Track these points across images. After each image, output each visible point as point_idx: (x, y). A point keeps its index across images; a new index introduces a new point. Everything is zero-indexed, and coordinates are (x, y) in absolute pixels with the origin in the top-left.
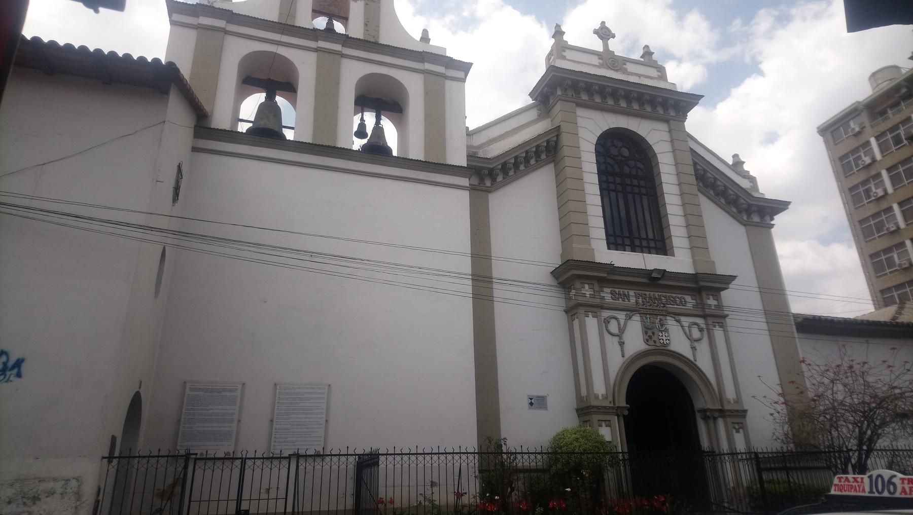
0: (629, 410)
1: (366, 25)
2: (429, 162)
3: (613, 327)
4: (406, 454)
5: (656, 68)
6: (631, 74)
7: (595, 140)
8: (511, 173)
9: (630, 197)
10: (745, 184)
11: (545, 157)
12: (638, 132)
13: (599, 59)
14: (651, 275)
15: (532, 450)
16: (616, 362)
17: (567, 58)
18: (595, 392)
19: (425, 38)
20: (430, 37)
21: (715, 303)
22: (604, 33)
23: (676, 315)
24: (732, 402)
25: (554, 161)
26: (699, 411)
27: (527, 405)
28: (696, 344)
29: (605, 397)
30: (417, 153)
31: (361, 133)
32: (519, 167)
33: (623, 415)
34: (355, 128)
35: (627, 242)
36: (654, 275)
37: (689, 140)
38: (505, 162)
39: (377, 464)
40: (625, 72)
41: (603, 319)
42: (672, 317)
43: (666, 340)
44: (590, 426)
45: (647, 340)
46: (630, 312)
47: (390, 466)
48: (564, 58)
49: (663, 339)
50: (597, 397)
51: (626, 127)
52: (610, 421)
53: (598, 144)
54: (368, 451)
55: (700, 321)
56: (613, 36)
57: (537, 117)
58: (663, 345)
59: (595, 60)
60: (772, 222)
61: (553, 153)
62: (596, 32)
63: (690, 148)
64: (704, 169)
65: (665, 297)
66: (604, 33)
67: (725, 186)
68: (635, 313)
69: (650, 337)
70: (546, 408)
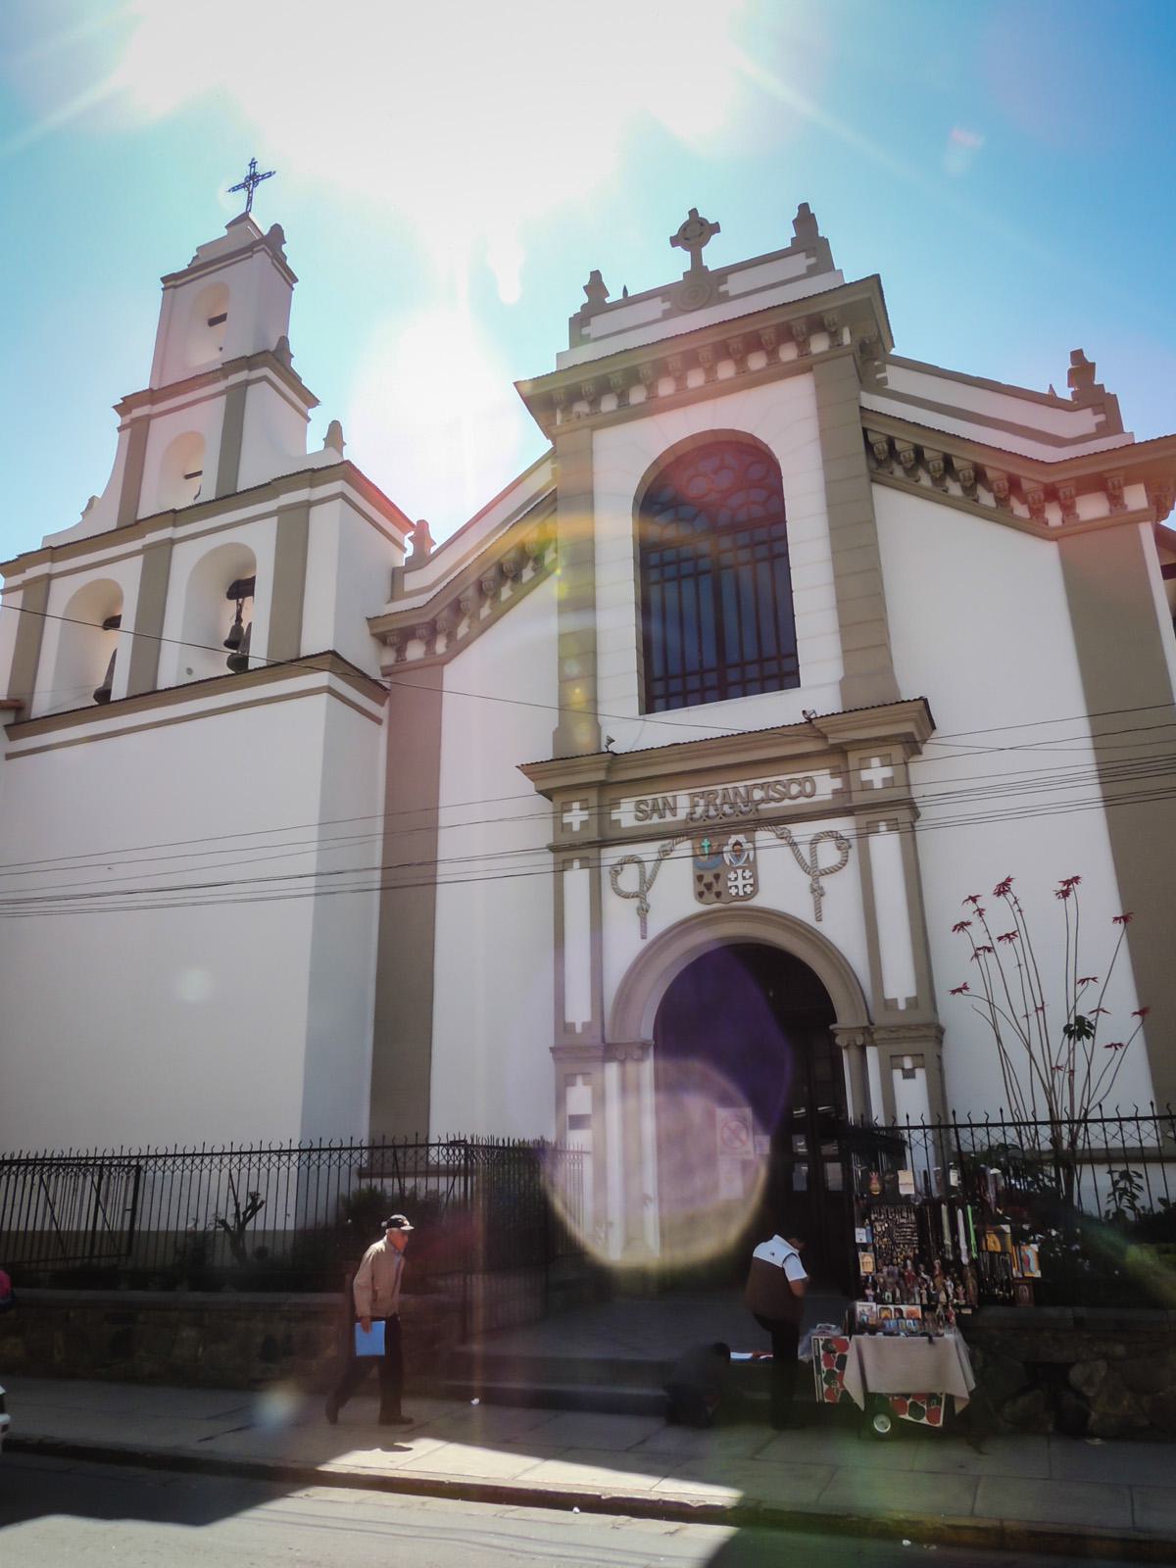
3: (629, 879)
13: (663, 302)
17: (592, 337)
18: (569, 1019)
19: (335, 435)
21: (887, 772)
22: (695, 232)
24: (902, 1006)
28: (825, 881)
29: (586, 1026)
34: (226, 635)
43: (745, 886)
45: (701, 895)
49: (736, 887)
55: (843, 825)
56: (716, 228)
59: (658, 307)
62: (674, 241)
65: (762, 786)
68: (678, 839)
69: (709, 886)
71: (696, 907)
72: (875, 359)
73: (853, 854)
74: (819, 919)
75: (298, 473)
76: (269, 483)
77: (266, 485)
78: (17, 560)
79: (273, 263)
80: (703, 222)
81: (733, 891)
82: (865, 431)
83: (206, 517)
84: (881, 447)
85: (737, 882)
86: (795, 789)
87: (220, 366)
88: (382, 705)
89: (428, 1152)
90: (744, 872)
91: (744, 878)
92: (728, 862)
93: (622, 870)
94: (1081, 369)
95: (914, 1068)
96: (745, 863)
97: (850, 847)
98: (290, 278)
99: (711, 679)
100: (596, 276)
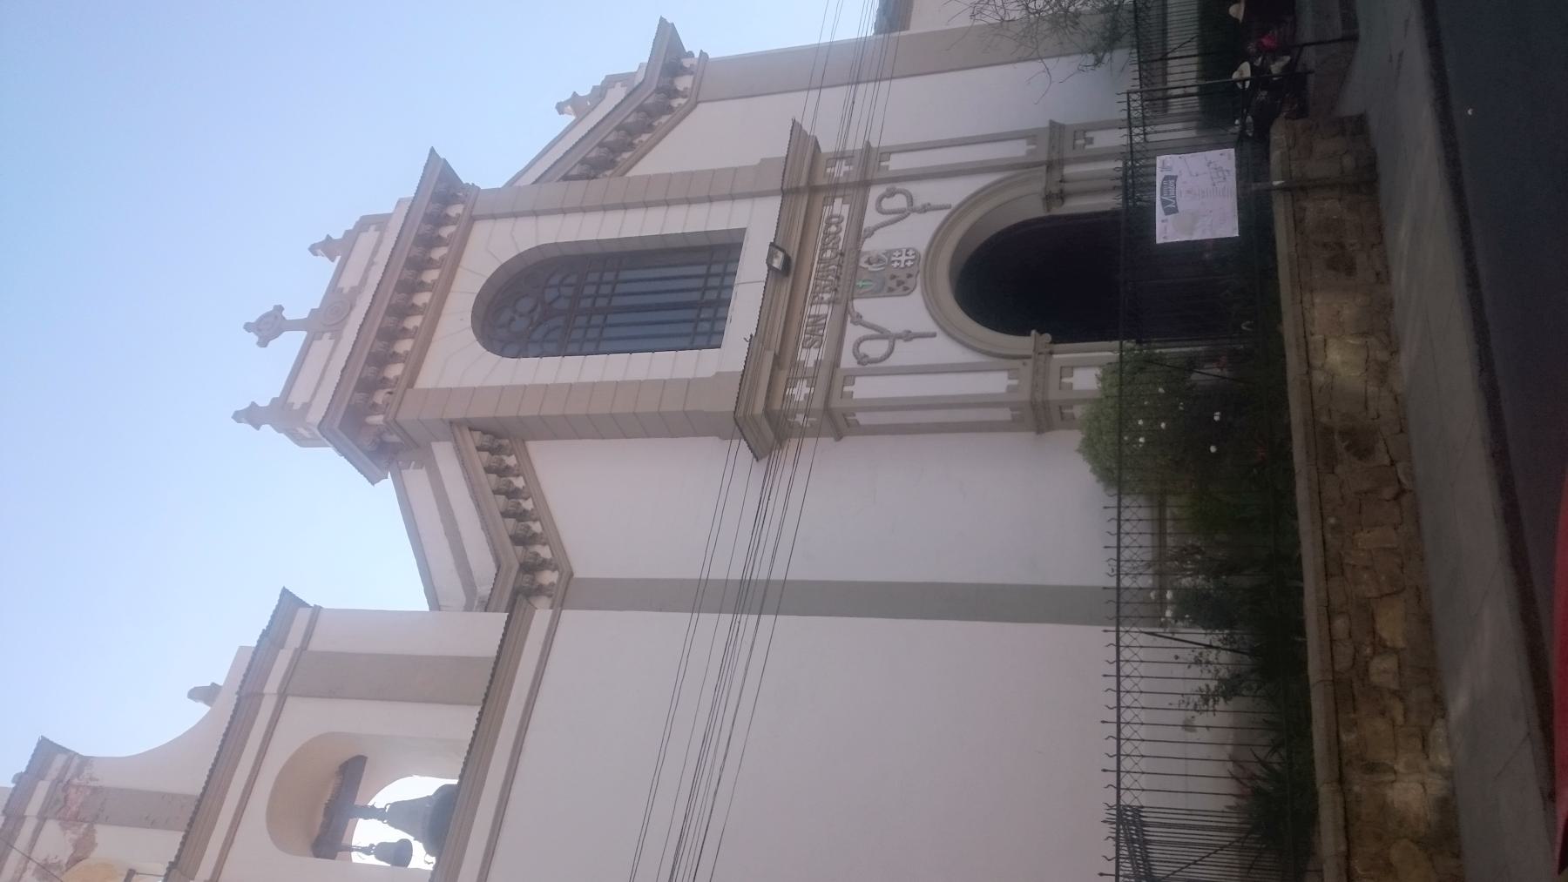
0: (1041, 332)
2: (487, 695)
3: (875, 349)
4: (1119, 747)
8: (536, 527)
9: (617, 301)
10: (617, 94)
11: (513, 456)
12: (489, 276)
13: (320, 338)
14: (776, 270)
15: (1114, 502)
16: (945, 350)
17: (307, 401)
18: (1003, 390)
19: (206, 694)
20: (209, 684)
23: (859, 234)
25: (523, 441)
26: (1049, 210)
28: (918, 204)
29: (1013, 373)
30: (463, 721)
31: (399, 855)
32: (525, 511)
33: (1051, 343)
35: (706, 314)
36: (777, 263)
37: (517, 184)
38: (511, 537)
39: (1137, 811)
40: (356, 291)
41: (861, 366)
42: (863, 242)
43: (907, 255)
44: (1071, 407)
45: (906, 289)
46: (846, 314)
47: (1144, 781)
49: (906, 261)
50: (1010, 389)
51: (475, 295)
52: (1061, 368)
53: (502, 353)
54: (1109, 830)
55: (875, 192)
56: (280, 309)
57: (424, 468)
58: (917, 261)
59: (323, 345)
60: (697, 55)
61: (505, 442)
62: (263, 343)
63: (537, 181)
64: (579, 162)
66: (269, 327)
67: (618, 129)
69: (900, 283)
71: (917, 297)
74: (949, 207)
76: (239, 700)
77: (237, 705)
80: (267, 315)
83: (207, 840)
86: (833, 229)
89: (1127, 589)
91: (899, 256)
92: (882, 268)
94: (576, 105)
95: (1085, 138)
100: (238, 416)
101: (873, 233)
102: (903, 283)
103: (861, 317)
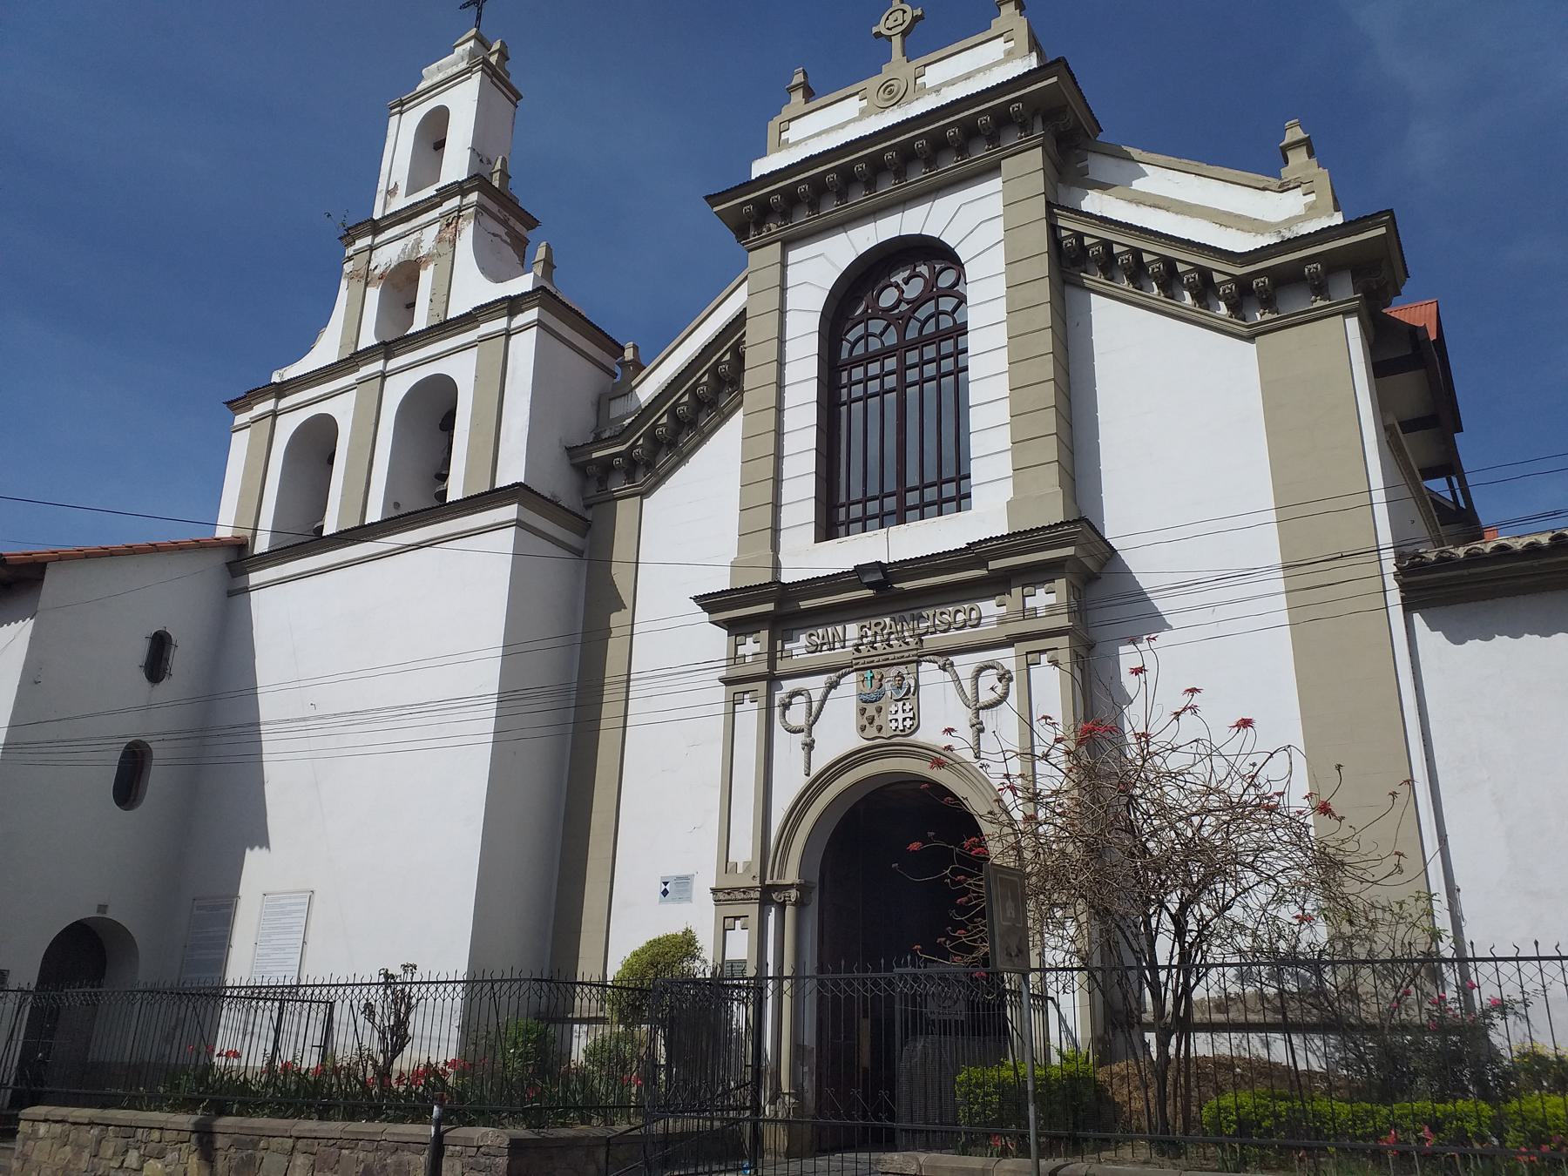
1: (431, 301)
3: (797, 715)
5: (1001, 35)
6: (937, 90)
7: (818, 300)
23: (945, 655)
27: (659, 894)
29: (748, 866)
42: (930, 661)
43: (904, 719)
45: (863, 729)
48: (782, 145)
49: (896, 720)
58: (898, 732)
68: (848, 670)
69: (871, 720)
70: (689, 899)
71: (856, 742)
72: (1077, 147)
73: (1013, 685)
75: (497, 301)
76: (469, 313)
78: (245, 397)
79: (492, 81)
81: (894, 725)
82: (1053, 229)
84: (1069, 243)
85: (894, 715)
86: (960, 617)
87: (436, 192)
88: (584, 536)
90: (904, 704)
91: (904, 711)
93: (790, 704)
96: (906, 694)
97: (1011, 679)
98: (515, 96)
99: (890, 504)
101: (945, 670)
102: (870, 723)
103: (835, 687)
